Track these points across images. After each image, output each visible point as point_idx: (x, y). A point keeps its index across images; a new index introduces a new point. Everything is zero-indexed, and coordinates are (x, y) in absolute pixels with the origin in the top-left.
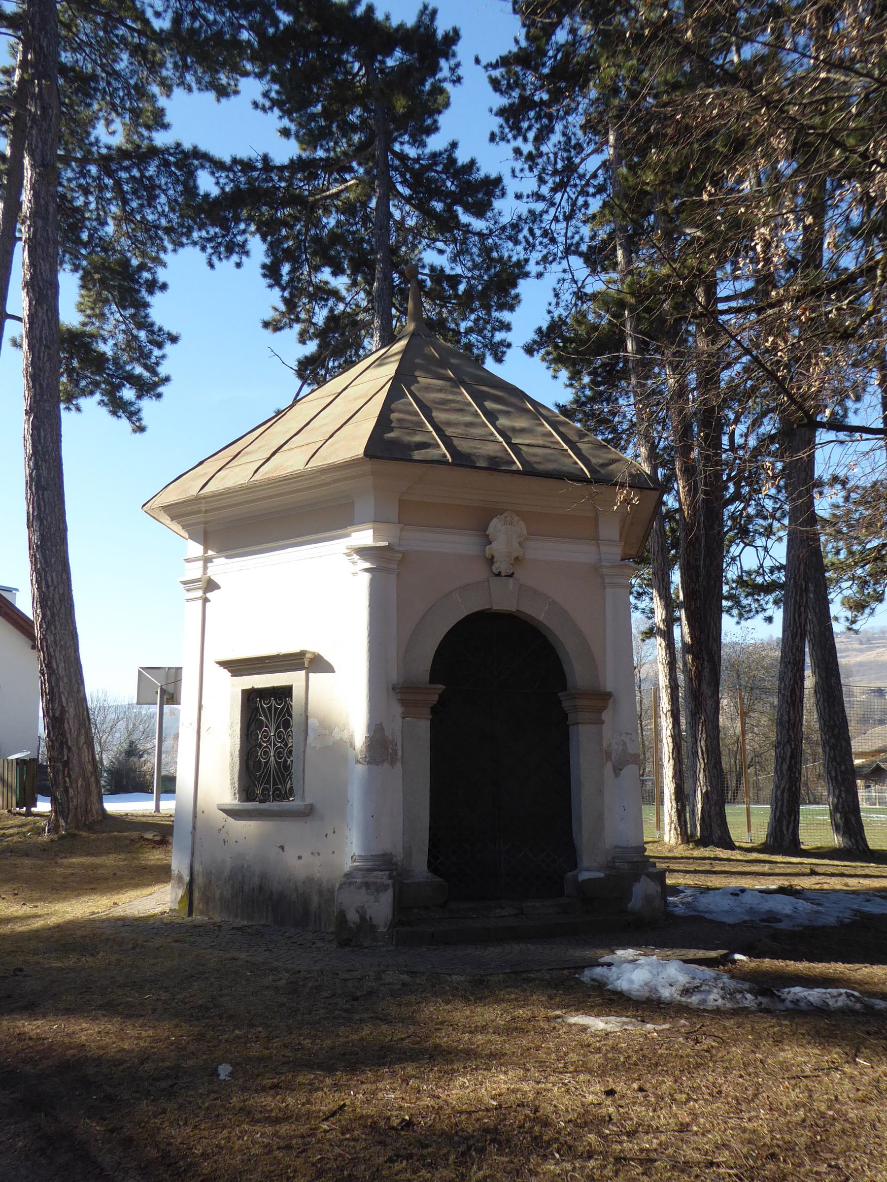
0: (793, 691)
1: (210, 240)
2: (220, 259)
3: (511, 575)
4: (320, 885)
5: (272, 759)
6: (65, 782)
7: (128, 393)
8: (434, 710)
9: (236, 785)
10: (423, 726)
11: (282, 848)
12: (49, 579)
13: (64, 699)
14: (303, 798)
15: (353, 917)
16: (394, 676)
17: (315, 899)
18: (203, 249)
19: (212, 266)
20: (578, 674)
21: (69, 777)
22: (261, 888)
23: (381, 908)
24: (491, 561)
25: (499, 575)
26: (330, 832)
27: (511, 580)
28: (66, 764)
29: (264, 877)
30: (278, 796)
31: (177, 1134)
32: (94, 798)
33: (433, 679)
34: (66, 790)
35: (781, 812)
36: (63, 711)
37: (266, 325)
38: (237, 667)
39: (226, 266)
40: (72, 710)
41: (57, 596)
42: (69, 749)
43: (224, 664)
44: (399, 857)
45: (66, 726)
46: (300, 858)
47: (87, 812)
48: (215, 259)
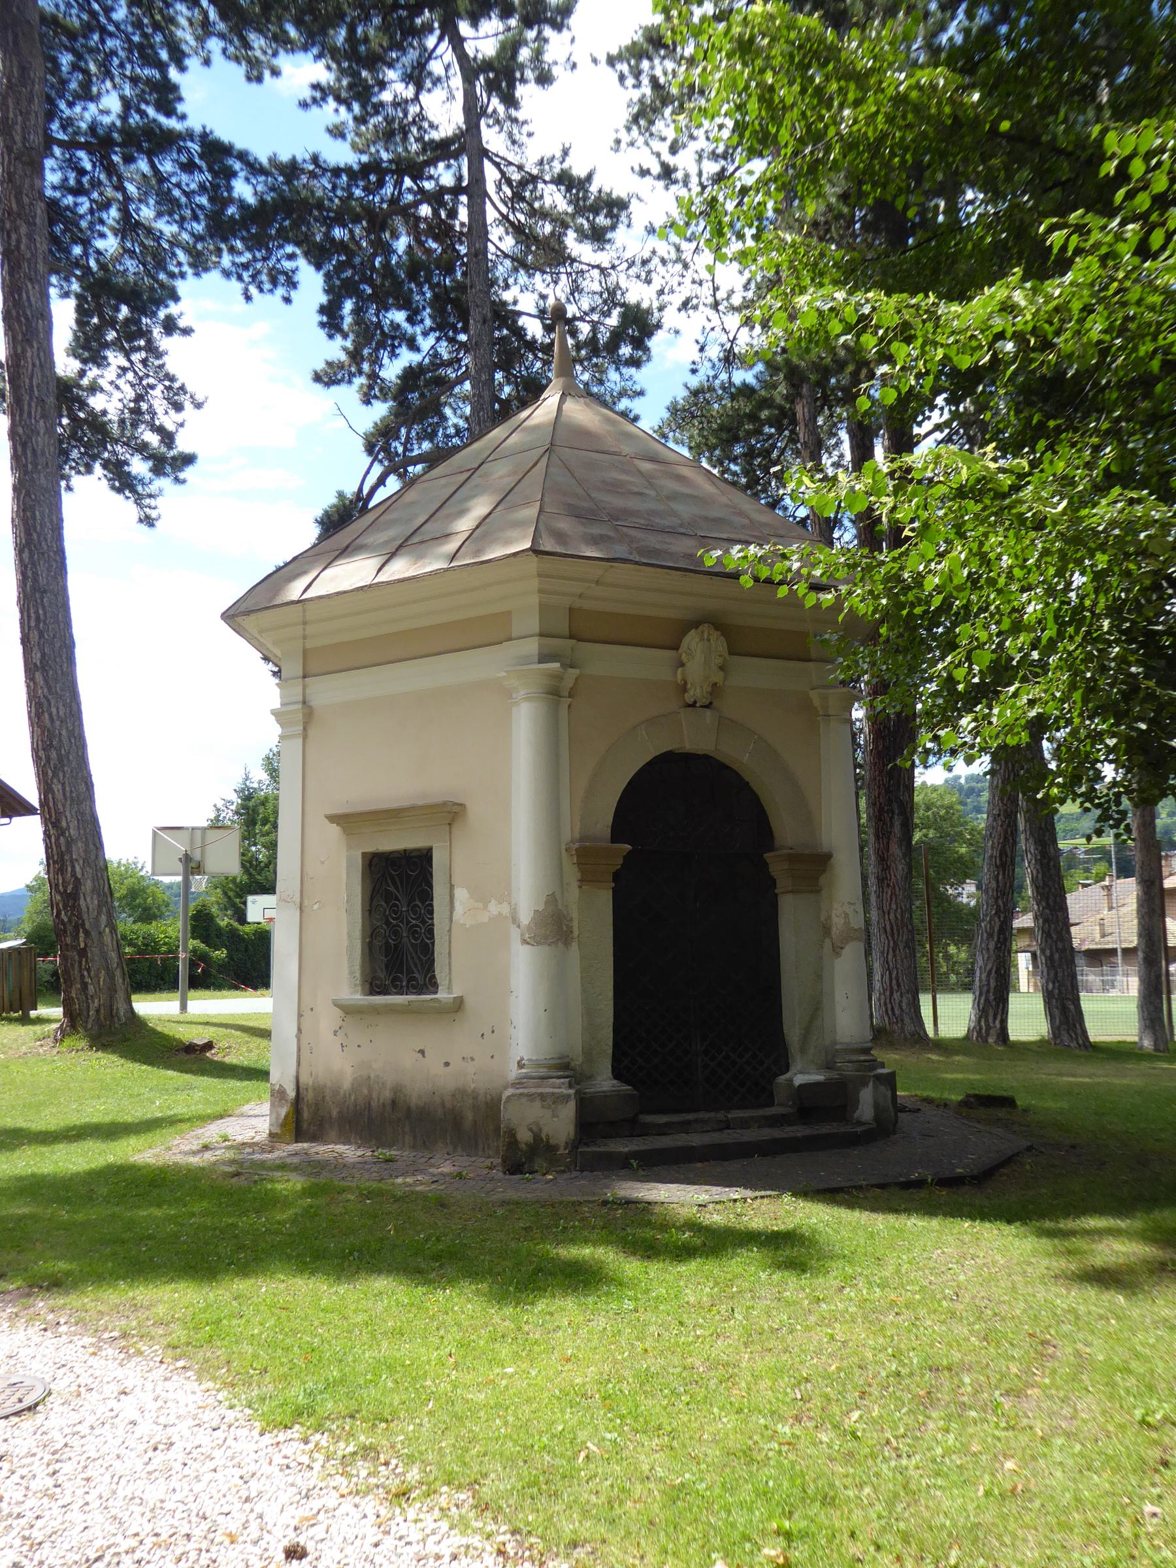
0: (1003, 853)
1: (245, 266)
2: (261, 290)
3: (708, 706)
4: (475, 1098)
5: (405, 940)
6: (82, 976)
7: (139, 466)
8: (616, 876)
9: (358, 974)
10: (604, 900)
11: (422, 1052)
12: (54, 710)
13: (78, 869)
14: (449, 989)
15: (524, 1136)
16: (567, 836)
17: (469, 1116)
18: (240, 278)
19: (248, 298)
20: (786, 830)
21: (89, 971)
22: (394, 1103)
23: (560, 1124)
24: (684, 689)
25: (693, 705)
26: (487, 1033)
27: (708, 712)
28: (83, 953)
29: (397, 1090)
30: (414, 987)
31: (1161, 1253)
32: (120, 995)
33: (615, 838)
34: (85, 986)
35: (987, 1000)
36: (77, 883)
37: (317, 378)
38: (348, 822)
39: (269, 301)
40: (89, 883)
41: (64, 732)
42: (87, 933)
43: (333, 819)
44: (578, 1061)
45: (82, 902)
46: (447, 1064)
47: (112, 1014)
48: (253, 290)
